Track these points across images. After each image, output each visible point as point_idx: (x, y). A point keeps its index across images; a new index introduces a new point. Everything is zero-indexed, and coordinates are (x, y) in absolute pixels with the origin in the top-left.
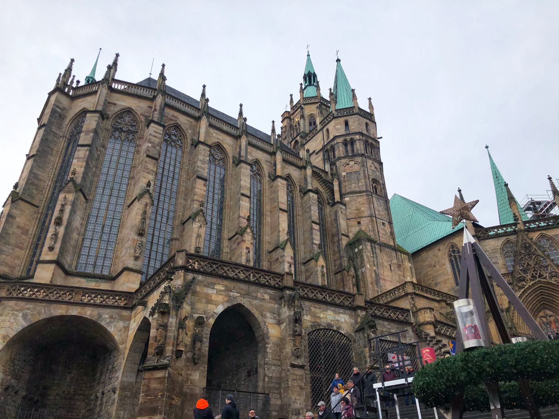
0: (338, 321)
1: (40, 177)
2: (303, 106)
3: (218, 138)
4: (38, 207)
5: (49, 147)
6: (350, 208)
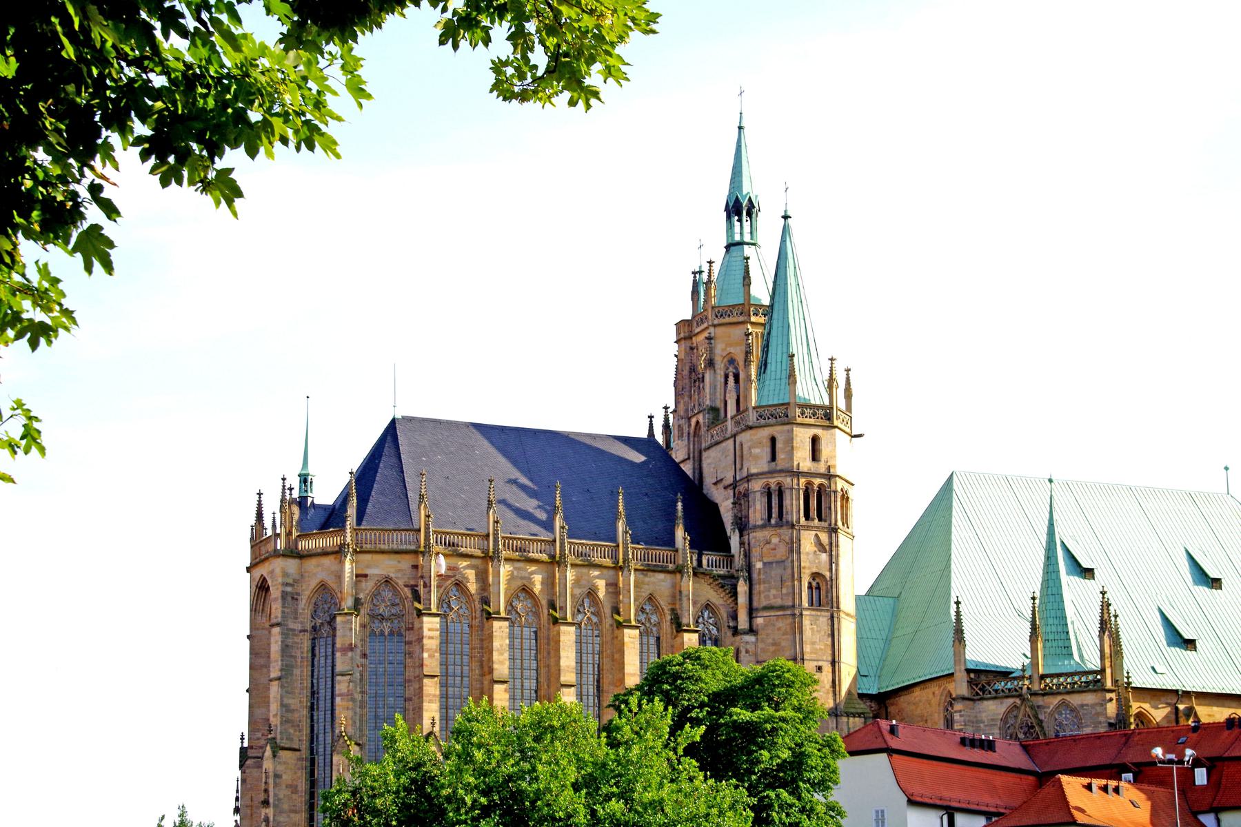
1: (293, 707)
2: (712, 330)
3: (522, 578)
4: (299, 750)
5: (292, 656)
6: (763, 641)
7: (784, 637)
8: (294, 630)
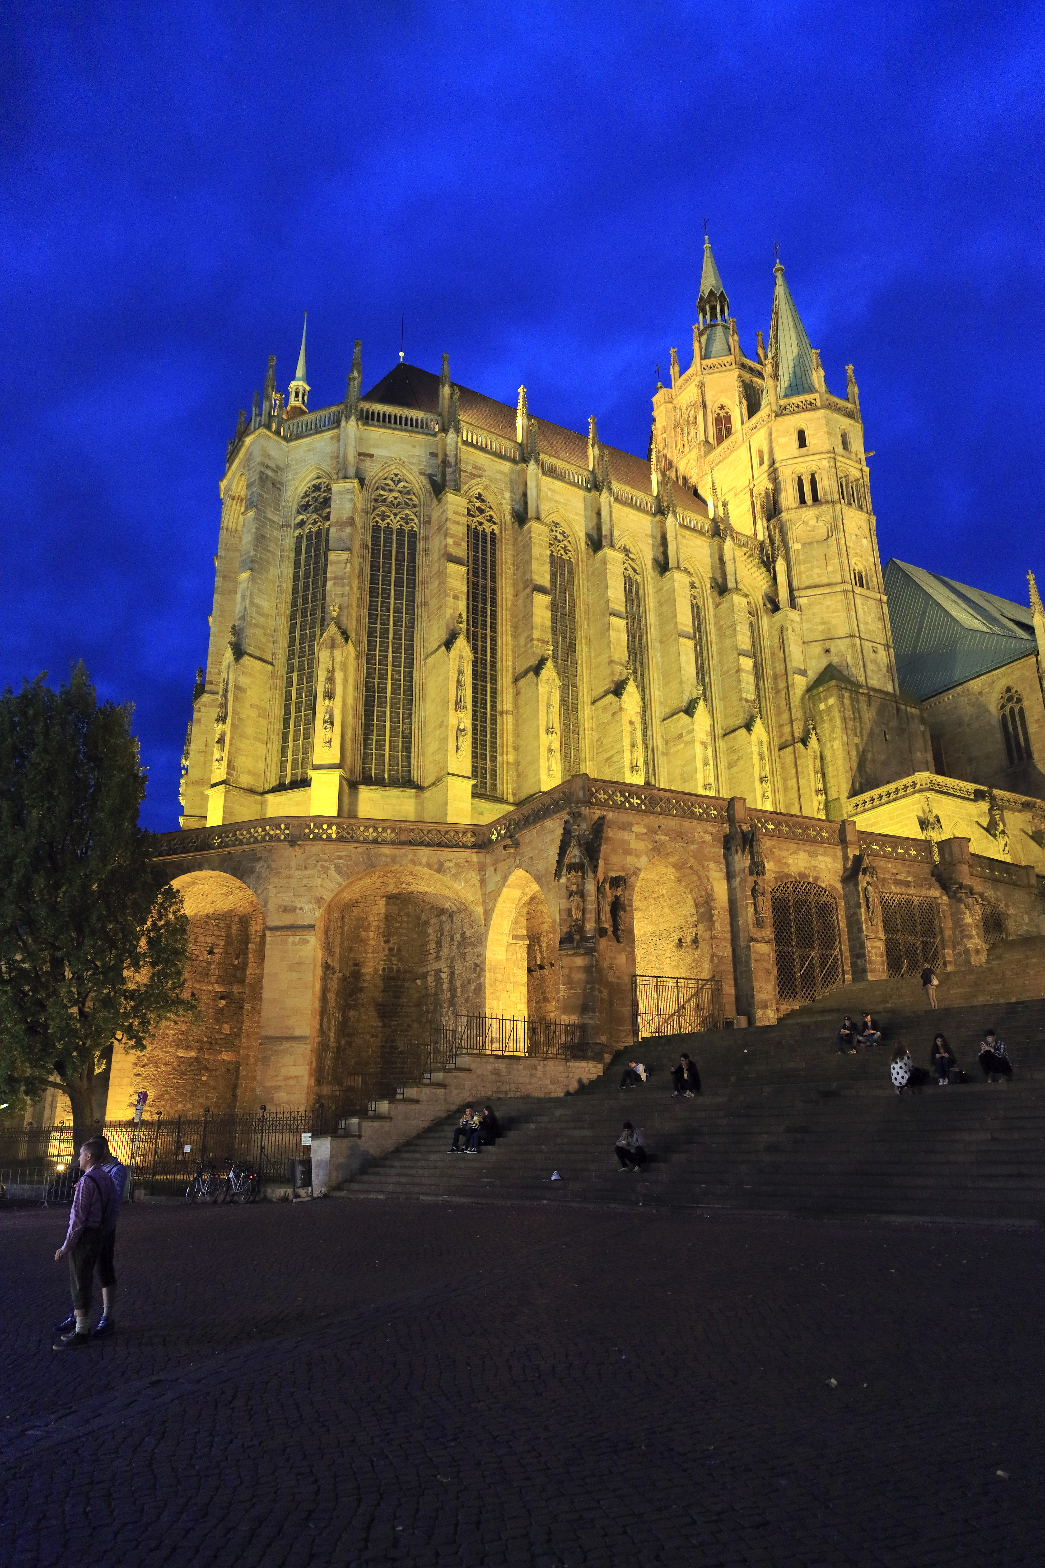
0: (815, 867)
6: (808, 621)
7: (834, 615)
8: (270, 520)
